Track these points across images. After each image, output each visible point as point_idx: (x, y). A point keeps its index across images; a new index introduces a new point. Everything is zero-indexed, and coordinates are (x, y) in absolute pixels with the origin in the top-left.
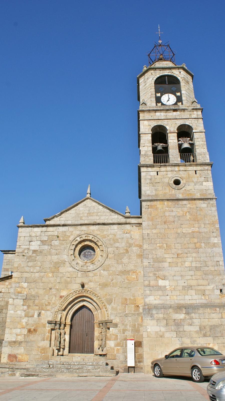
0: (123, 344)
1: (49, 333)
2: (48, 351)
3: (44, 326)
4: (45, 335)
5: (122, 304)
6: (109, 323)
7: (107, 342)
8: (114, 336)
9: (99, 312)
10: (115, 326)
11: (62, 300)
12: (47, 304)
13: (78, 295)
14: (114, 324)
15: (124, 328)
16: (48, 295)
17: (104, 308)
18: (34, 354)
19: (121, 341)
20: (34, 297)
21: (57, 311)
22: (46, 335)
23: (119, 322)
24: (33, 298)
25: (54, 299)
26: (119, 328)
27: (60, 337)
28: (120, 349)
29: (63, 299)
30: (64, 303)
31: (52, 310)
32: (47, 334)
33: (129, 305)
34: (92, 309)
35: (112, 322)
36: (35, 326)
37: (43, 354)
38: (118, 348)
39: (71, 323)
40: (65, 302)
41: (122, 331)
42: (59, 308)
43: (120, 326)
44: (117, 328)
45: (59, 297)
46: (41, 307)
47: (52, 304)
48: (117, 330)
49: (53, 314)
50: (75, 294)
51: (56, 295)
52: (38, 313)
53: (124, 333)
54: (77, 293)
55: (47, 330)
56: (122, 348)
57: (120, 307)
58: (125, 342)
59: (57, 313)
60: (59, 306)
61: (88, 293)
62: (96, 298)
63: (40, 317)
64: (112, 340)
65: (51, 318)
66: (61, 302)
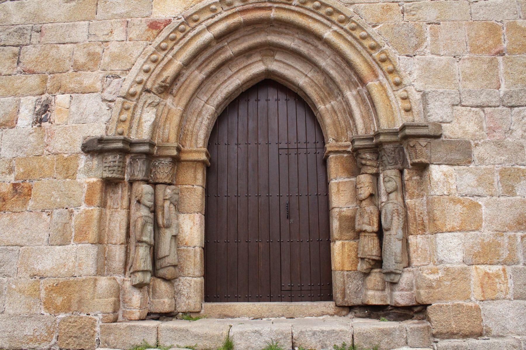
0: (512, 250)
1: (89, 202)
2: (89, 296)
3: (68, 170)
4: (72, 212)
5: (475, 49)
6: (423, 142)
7: (412, 239)
8: (459, 207)
9: (353, 95)
10: (457, 157)
11: (159, 40)
12: (82, 60)
13: (239, 18)
14: (450, 142)
15: (507, 166)
16: (87, 22)
17: (380, 72)
18: (11, 312)
19: (500, 233)
20: (21, 32)
21: (132, 90)
22: (76, 212)
23: (474, 135)
24: (13, 41)
25: (119, 34)
26: (483, 167)
27: (150, 220)
28: (498, 276)
29: (165, 33)
30: (170, 56)
31: (109, 89)
33: (511, 53)
34: (312, 86)
35: (438, 137)
36: (22, 170)
37: (62, 316)
38: (486, 273)
39: (207, 155)
40: (176, 48)
41: (497, 178)
42: (144, 77)
43: (486, 156)
44: (472, 166)
45: (145, 26)
46: (49, 76)
47: (106, 59)
48: (468, 174)
49: (110, 108)
50: (225, 14)
51: (129, 20)
52: (38, 107)
53: (510, 191)
54: (237, 9)
55: (80, 185)
56: (509, 269)
57: (468, 64)
58: (522, 238)
59: (131, 104)
60: (146, 67)
61: (293, 8)
62: (335, 28)
63: (45, 125)
64: (448, 227)
65: (104, 126)
66: (151, 49)
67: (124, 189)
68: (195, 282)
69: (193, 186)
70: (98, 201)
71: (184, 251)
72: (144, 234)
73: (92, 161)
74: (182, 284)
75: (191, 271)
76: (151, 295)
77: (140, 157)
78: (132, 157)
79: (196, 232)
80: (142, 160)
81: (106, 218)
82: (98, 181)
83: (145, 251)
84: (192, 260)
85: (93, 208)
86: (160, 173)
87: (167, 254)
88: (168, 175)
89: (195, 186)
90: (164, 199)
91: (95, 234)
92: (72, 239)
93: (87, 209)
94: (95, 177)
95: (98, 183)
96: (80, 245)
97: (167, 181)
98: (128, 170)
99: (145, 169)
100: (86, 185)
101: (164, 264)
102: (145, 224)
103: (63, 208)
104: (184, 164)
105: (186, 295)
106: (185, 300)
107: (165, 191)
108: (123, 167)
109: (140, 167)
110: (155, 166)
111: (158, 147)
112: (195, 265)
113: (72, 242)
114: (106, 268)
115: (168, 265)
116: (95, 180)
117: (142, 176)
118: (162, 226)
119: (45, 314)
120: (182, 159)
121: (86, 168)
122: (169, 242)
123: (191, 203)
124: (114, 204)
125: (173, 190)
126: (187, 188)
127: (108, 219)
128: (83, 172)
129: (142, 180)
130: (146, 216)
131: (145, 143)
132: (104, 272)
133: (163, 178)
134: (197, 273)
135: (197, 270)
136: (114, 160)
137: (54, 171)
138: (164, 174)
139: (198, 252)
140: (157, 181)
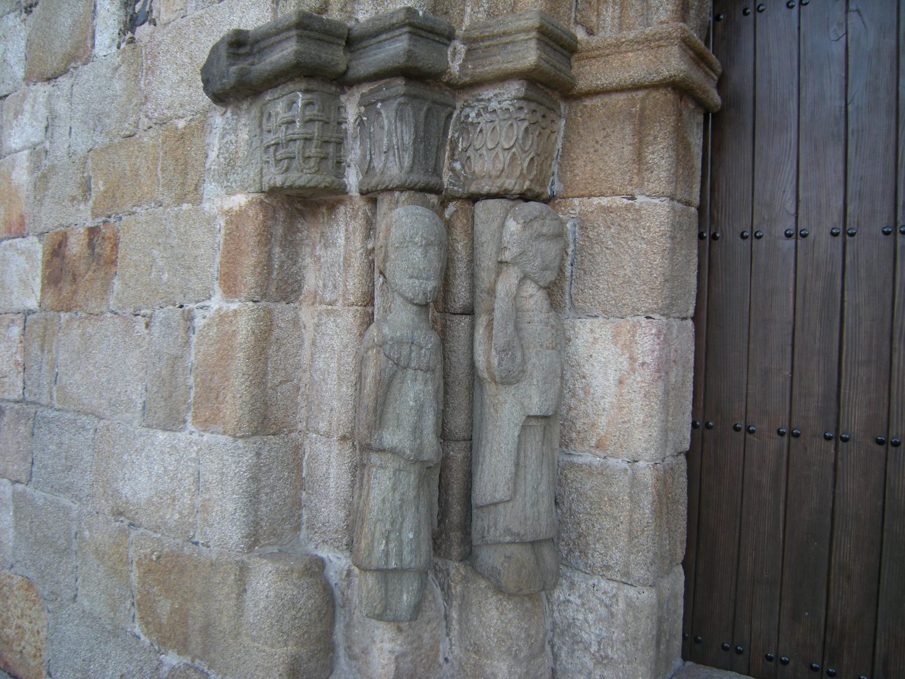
4: (189, 318)
32: (217, 302)
63: (144, 31)
67: (351, 229)
68: (630, 604)
69: (633, 198)
70: (250, 280)
71: (591, 474)
72: (390, 415)
73: (235, 130)
74: (579, 601)
75: (616, 556)
76: (455, 633)
77: (388, 93)
78: (363, 95)
79: (638, 402)
80: (395, 104)
81: (300, 337)
82: (251, 203)
83: (394, 489)
84: (624, 517)
85: (234, 306)
86: (484, 151)
87: (501, 494)
88: (513, 158)
89: (640, 199)
90: (501, 262)
91: (239, 402)
92: (190, 414)
93: (225, 306)
94: (244, 189)
95: (251, 213)
96: (207, 437)
97: (510, 183)
98: (354, 153)
99: (408, 139)
100: (221, 222)
101: (492, 530)
102: (393, 377)
103: (174, 305)
104: (594, 107)
105: (594, 648)
106: (590, 664)
107: (503, 225)
108: (327, 142)
109: (390, 134)
110: (465, 127)
111: (467, 41)
112: (631, 536)
113: (190, 426)
114: (305, 517)
115: (508, 539)
116: (240, 200)
117: (402, 167)
118: (486, 375)
119: (143, 638)
120: (582, 85)
121: (222, 160)
122: (512, 446)
123: (622, 273)
124: (325, 286)
125: (527, 224)
126: (607, 210)
127: (307, 344)
128: (217, 177)
129: (402, 188)
130: (400, 342)
131: (392, 28)
132: (298, 528)
133: (494, 173)
134: (639, 573)
135: (640, 557)
136: (288, 116)
137: (158, 180)
138: (497, 156)
139: (646, 486)
140: (473, 188)
